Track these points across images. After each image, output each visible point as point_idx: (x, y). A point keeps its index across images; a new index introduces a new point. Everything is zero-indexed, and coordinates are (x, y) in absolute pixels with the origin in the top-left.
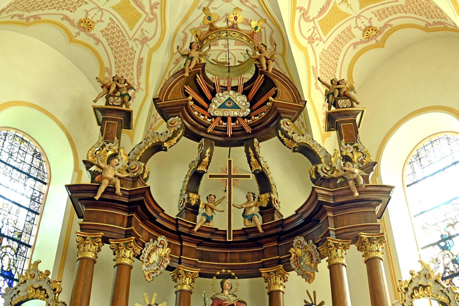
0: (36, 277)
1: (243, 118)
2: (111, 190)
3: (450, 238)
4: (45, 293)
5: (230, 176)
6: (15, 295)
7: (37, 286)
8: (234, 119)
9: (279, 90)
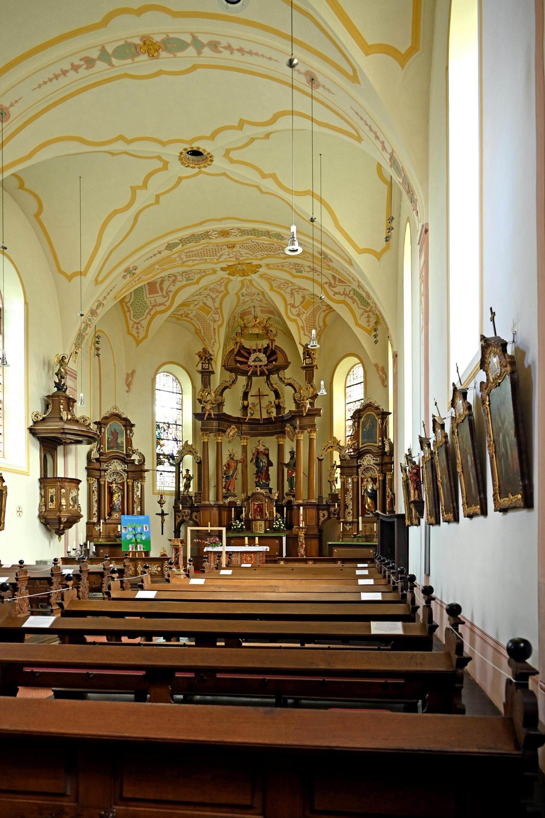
1: (265, 366)
2: (210, 414)
5: (260, 396)
8: (260, 366)
9: (278, 357)
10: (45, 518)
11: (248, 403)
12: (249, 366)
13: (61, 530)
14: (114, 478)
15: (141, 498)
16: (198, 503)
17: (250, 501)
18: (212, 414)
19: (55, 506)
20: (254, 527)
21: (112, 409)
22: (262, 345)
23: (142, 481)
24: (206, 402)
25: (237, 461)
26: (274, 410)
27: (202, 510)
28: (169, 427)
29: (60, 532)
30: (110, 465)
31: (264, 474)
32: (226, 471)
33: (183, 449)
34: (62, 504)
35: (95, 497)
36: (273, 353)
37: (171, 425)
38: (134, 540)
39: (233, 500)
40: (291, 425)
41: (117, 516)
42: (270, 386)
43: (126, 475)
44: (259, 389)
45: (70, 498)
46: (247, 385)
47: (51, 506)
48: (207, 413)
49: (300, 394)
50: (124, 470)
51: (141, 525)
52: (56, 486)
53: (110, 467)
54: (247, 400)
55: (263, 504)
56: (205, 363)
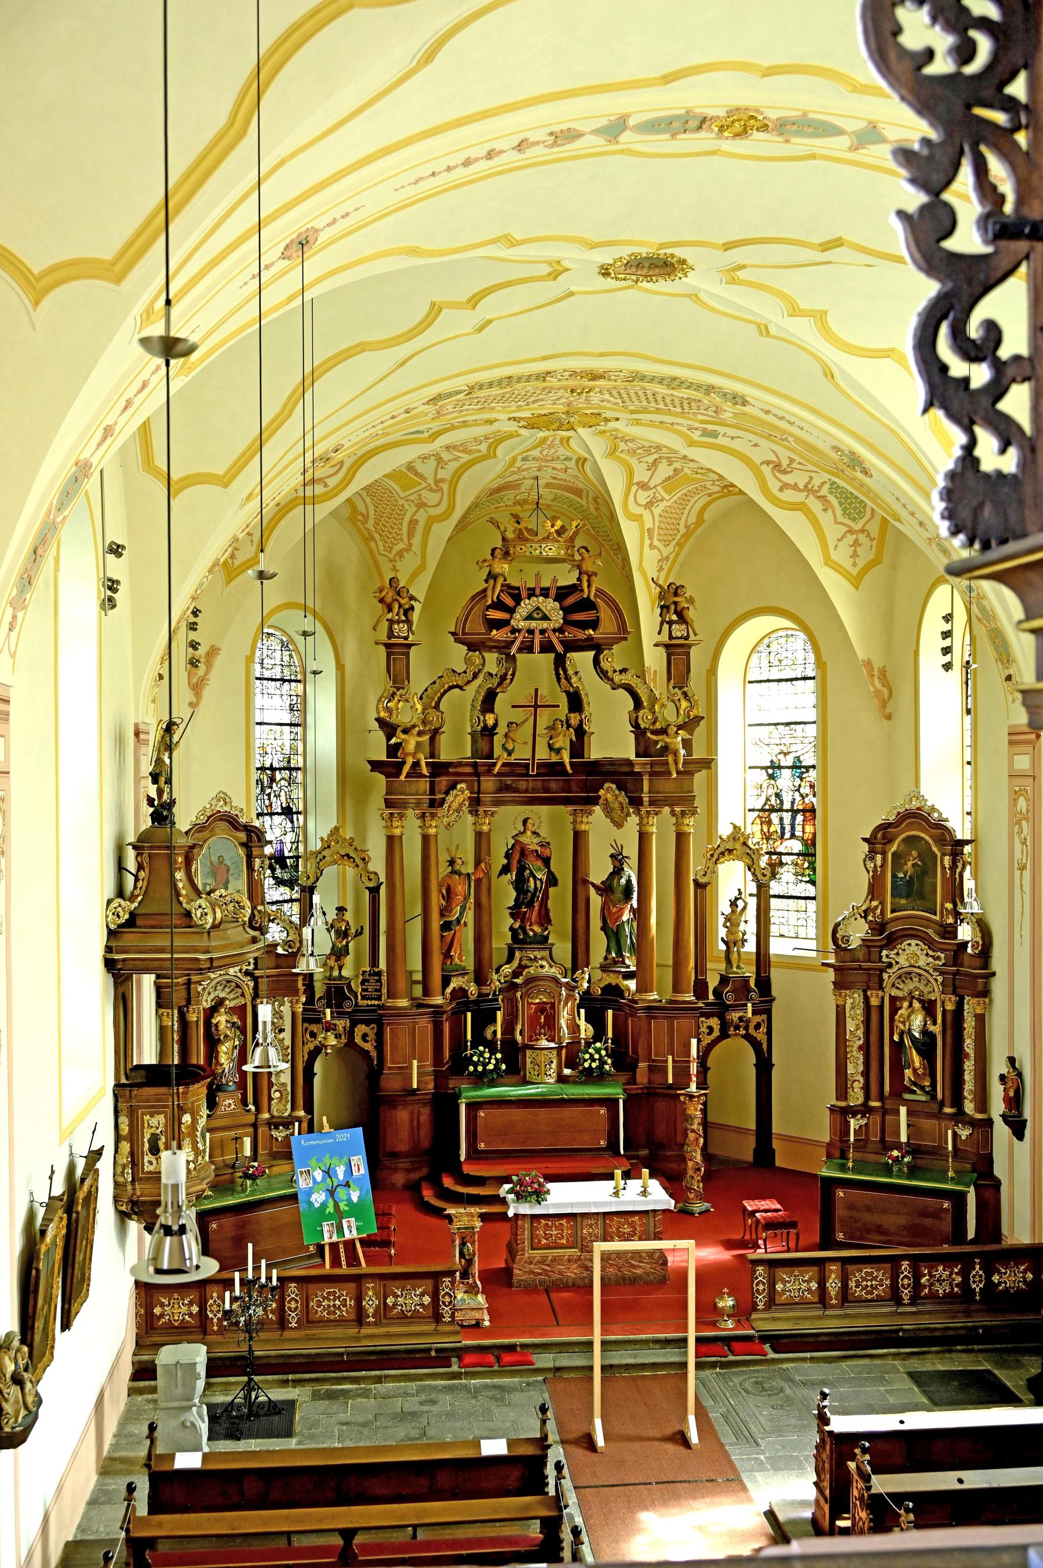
1: (554, 631)
2: (416, 764)
3: (780, 767)
8: (543, 632)
9: (602, 615)
11: (496, 720)
12: (514, 631)
14: (216, 994)
16: (371, 999)
17: (519, 994)
18: (423, 764)
20: (529, 1065)
21: (214, 802)
22: (555, 580)
24: (405, 731)
25: (468, 875)
26: (563, 741)
27: (389, 1024)
28: (272, 779)
31: (536, 908)
36: (588, 605)
37: (277, 772)
38: (330, 1209)
39: (460, 983)
40: (619, 788)
42: (563, 681)
43: (251, 984)
44: (536, 690)
46: (503, 678)
48: (410, 761)
49: (654, 713)
50: (247, 973)
52: (167, 1107)
54: (492, 711)
55: (553, 1005)
56: (399, 622)
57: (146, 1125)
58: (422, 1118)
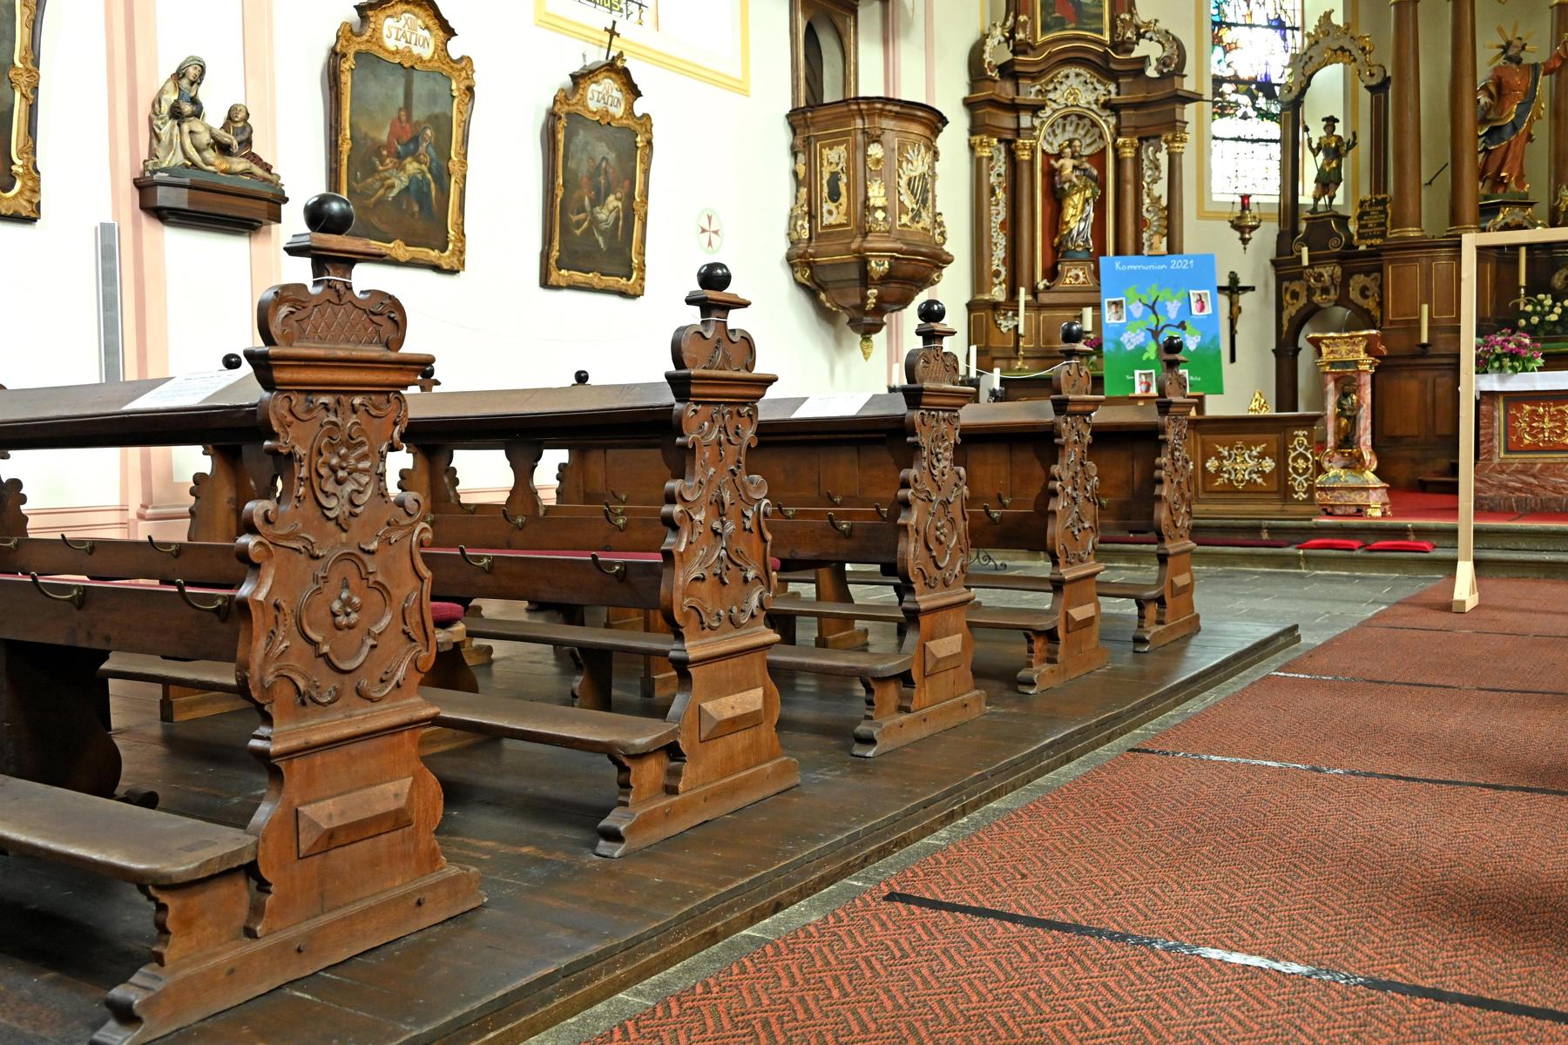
0: (1331, 34)
4: (1351, 55)
6: (1306, 63)
7: (1336, 47)
10: (810, 265)
13: (867, 313)
14: (1068, 135)
15: (1168, 207)
16: (1372, 237)
19: (847, 214)
23: (1174, 140)
25: (1535, 67)
27: (1391, 261)
29: (868, 320)
30: (1051, 87)
32: (1488, 108)
33: (1311, 46)
34: (872, 202)
35: (998, 213)
41: (1077, 277)
43: (1113, 121)
45: (903, 182)
47: (832, 215)
51: (1182, 293)
52: (848, 133)
53: (1051, 96)
57: (825, 163)
58: (1440, 391)
